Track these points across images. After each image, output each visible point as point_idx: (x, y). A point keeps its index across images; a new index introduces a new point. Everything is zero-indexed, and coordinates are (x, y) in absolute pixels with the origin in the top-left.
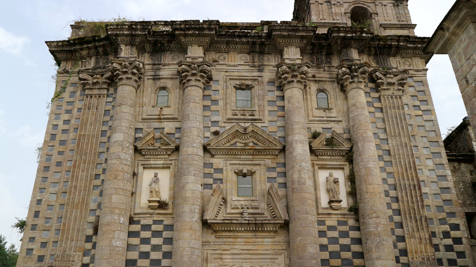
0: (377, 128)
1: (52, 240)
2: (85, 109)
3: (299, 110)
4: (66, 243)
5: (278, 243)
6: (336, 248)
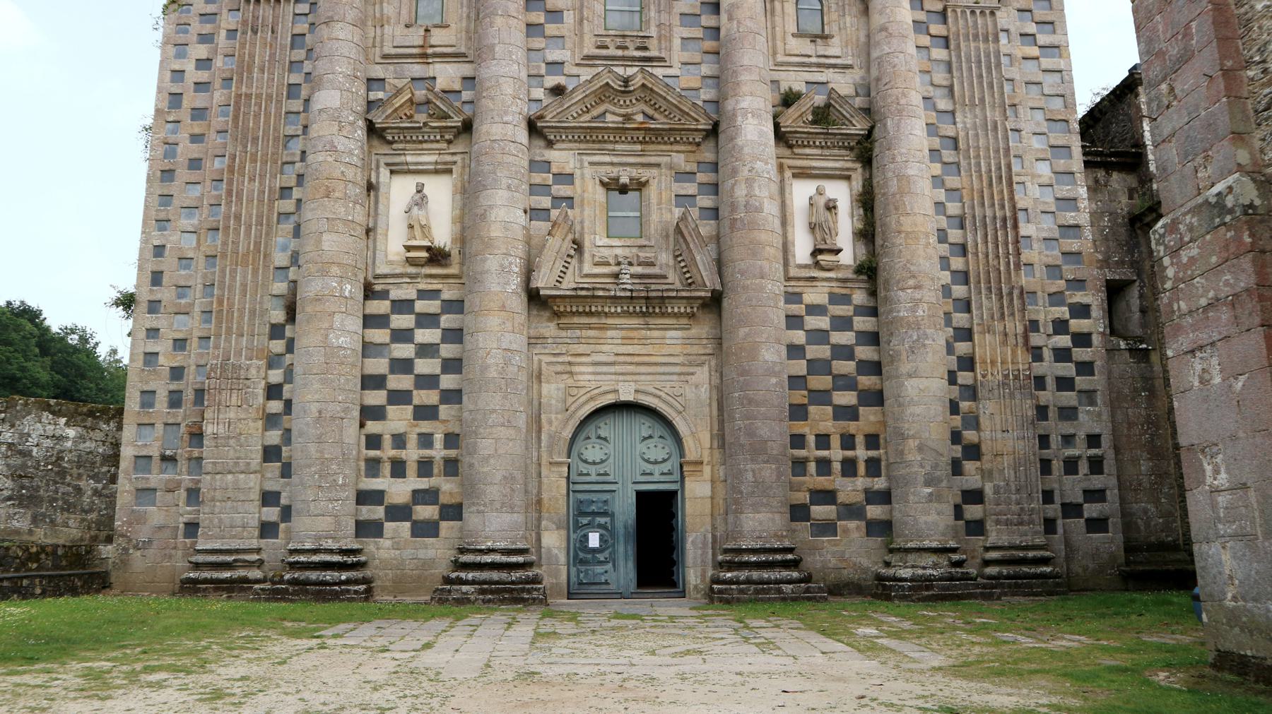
0: (932, 84)
1: (197, 333)
2: (244, 33)
3: (755, 38)
4: (228, 340)
5: (697, 341)
6: (823, 352)
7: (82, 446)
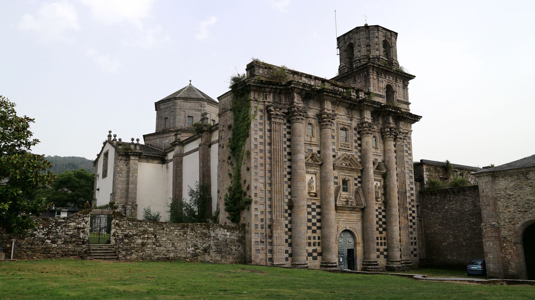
7: (231, 237)
